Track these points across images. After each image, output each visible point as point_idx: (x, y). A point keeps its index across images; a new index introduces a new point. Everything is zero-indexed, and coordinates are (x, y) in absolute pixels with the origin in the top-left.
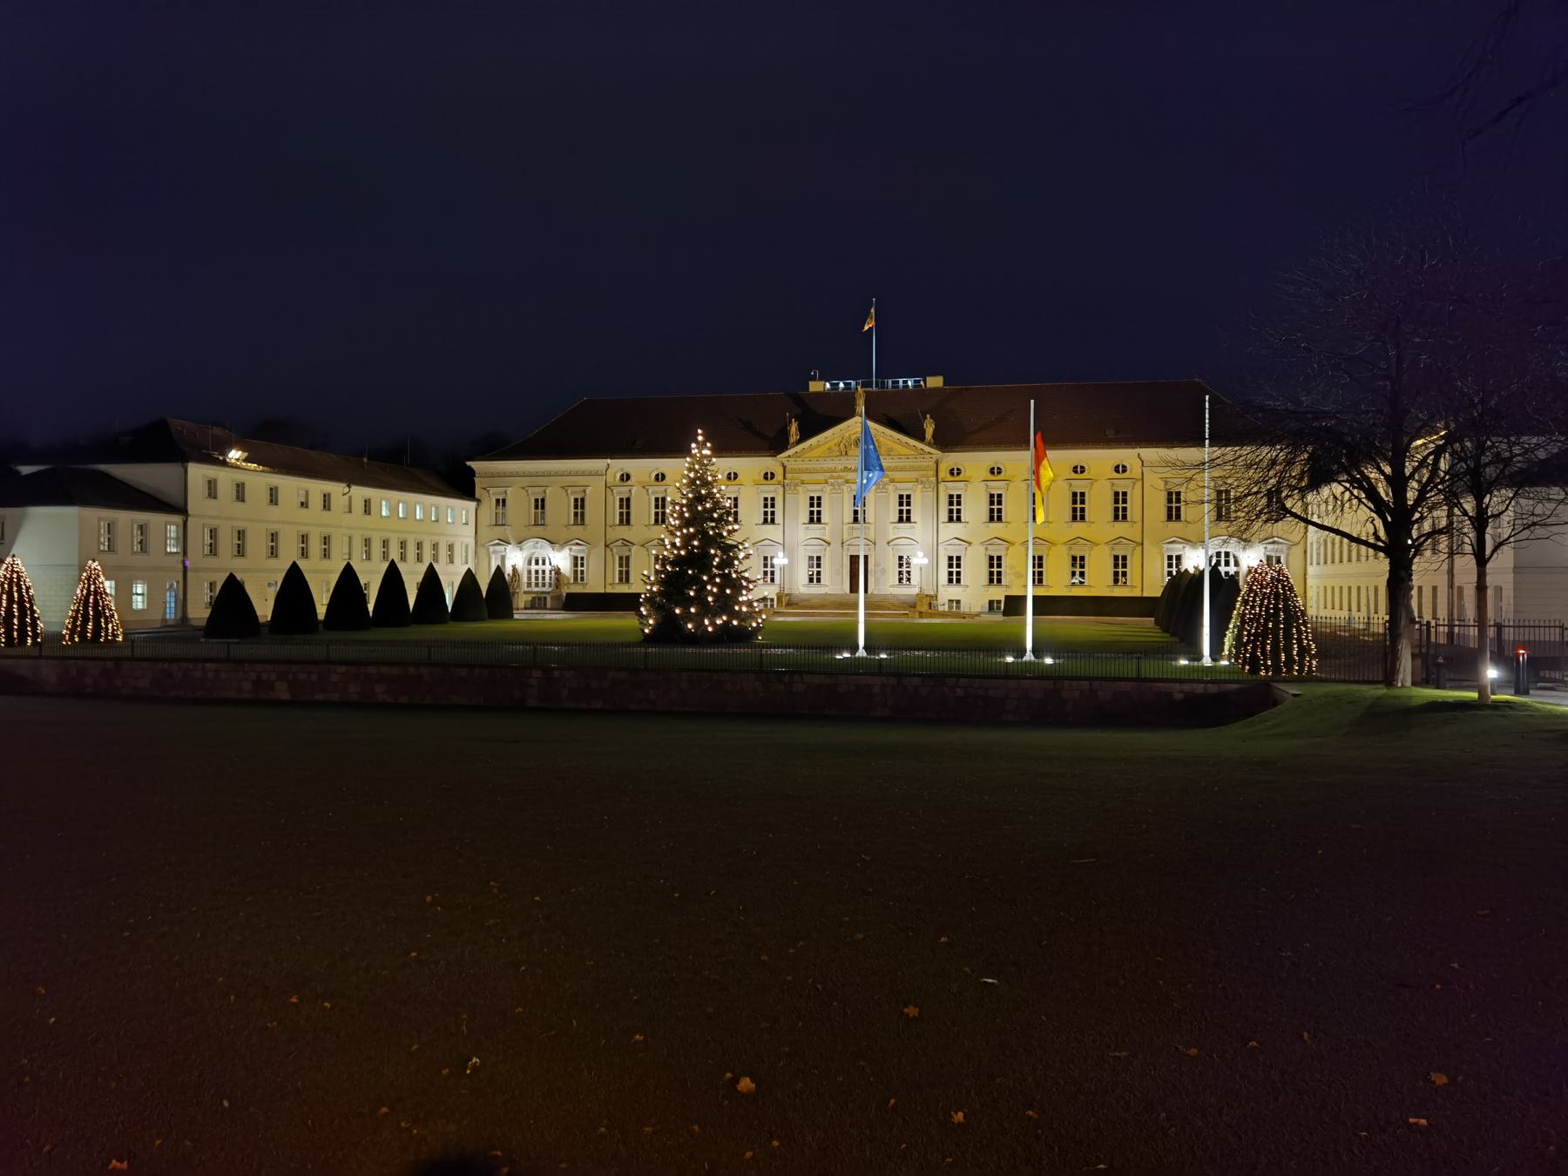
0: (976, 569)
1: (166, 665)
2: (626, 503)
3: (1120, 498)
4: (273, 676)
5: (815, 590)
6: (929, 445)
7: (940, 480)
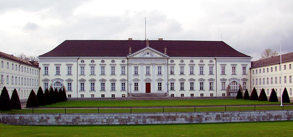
0: (177, 86)
1: (77, 115)
2: (83, 68)
3: (211, 68)
4: (114, 118)
5: (136, 92)
6: (166, 55)
7: (168, 64)
